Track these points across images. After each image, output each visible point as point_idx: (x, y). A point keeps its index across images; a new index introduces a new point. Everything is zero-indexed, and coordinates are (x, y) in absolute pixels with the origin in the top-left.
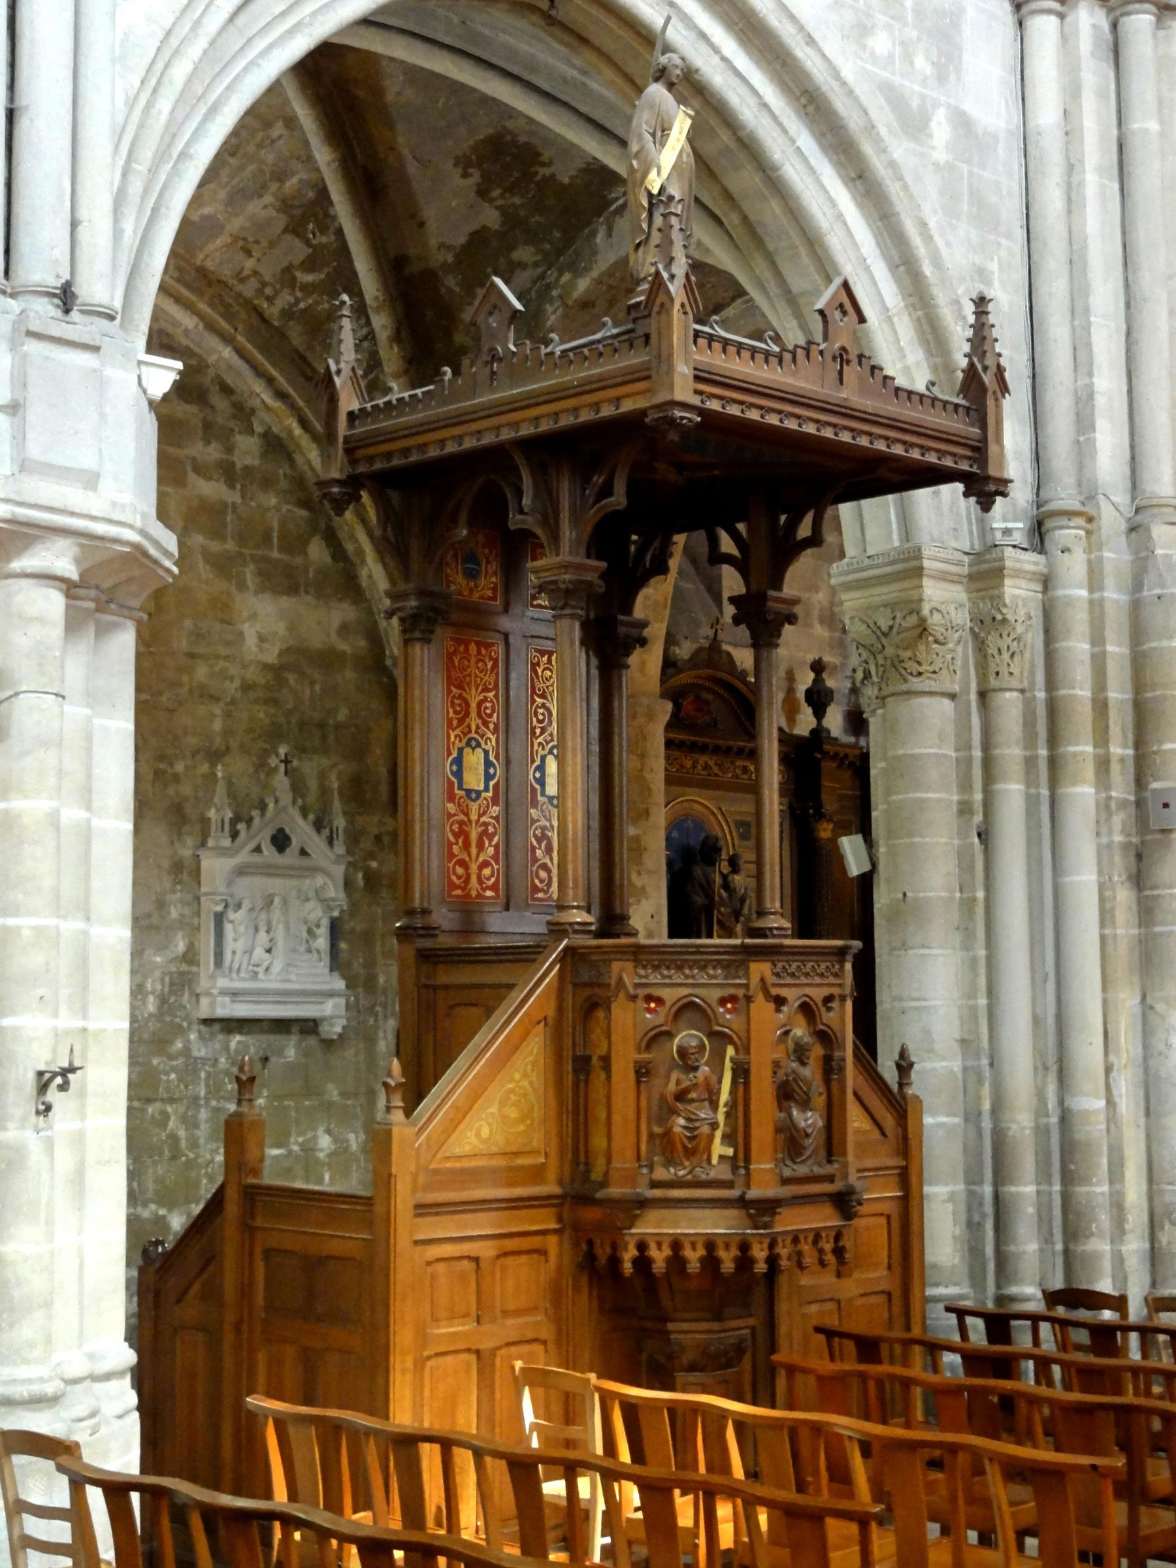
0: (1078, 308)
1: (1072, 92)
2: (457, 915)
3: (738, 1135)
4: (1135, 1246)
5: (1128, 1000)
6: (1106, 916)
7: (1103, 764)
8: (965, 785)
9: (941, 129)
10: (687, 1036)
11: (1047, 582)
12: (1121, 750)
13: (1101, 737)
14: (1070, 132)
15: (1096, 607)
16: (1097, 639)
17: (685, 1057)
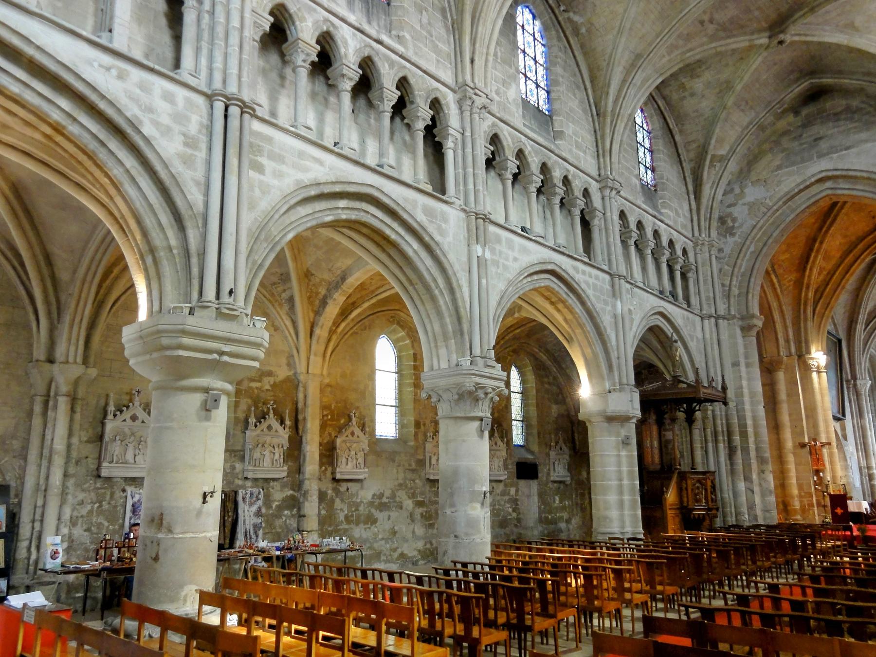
0: (715, 367)
1: (711, 332)
2: (659, 467)
3: (706, 498)
4: (734, 519)
5: (730, 479)
6: (726, 465)
7: (724, 441)
8: (702, 444)
9: (695, 340)
10: (698, 485)
11: (713, 411)
12: (726, 438)
13: (723, 436)
14: (711, 339)
15: (721, 415)
16: (722, 420)
17: (698, 488)
